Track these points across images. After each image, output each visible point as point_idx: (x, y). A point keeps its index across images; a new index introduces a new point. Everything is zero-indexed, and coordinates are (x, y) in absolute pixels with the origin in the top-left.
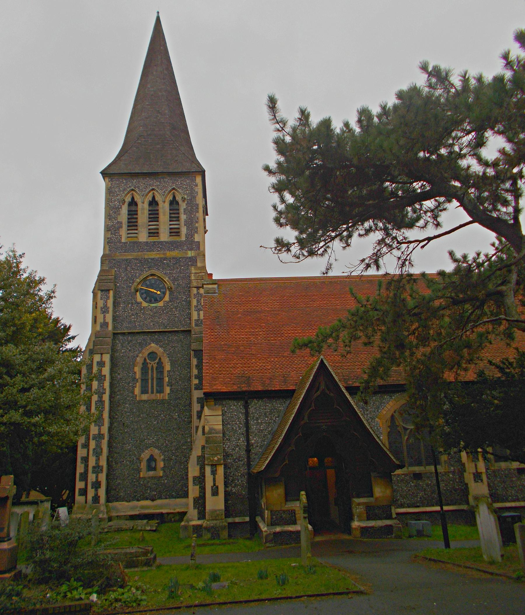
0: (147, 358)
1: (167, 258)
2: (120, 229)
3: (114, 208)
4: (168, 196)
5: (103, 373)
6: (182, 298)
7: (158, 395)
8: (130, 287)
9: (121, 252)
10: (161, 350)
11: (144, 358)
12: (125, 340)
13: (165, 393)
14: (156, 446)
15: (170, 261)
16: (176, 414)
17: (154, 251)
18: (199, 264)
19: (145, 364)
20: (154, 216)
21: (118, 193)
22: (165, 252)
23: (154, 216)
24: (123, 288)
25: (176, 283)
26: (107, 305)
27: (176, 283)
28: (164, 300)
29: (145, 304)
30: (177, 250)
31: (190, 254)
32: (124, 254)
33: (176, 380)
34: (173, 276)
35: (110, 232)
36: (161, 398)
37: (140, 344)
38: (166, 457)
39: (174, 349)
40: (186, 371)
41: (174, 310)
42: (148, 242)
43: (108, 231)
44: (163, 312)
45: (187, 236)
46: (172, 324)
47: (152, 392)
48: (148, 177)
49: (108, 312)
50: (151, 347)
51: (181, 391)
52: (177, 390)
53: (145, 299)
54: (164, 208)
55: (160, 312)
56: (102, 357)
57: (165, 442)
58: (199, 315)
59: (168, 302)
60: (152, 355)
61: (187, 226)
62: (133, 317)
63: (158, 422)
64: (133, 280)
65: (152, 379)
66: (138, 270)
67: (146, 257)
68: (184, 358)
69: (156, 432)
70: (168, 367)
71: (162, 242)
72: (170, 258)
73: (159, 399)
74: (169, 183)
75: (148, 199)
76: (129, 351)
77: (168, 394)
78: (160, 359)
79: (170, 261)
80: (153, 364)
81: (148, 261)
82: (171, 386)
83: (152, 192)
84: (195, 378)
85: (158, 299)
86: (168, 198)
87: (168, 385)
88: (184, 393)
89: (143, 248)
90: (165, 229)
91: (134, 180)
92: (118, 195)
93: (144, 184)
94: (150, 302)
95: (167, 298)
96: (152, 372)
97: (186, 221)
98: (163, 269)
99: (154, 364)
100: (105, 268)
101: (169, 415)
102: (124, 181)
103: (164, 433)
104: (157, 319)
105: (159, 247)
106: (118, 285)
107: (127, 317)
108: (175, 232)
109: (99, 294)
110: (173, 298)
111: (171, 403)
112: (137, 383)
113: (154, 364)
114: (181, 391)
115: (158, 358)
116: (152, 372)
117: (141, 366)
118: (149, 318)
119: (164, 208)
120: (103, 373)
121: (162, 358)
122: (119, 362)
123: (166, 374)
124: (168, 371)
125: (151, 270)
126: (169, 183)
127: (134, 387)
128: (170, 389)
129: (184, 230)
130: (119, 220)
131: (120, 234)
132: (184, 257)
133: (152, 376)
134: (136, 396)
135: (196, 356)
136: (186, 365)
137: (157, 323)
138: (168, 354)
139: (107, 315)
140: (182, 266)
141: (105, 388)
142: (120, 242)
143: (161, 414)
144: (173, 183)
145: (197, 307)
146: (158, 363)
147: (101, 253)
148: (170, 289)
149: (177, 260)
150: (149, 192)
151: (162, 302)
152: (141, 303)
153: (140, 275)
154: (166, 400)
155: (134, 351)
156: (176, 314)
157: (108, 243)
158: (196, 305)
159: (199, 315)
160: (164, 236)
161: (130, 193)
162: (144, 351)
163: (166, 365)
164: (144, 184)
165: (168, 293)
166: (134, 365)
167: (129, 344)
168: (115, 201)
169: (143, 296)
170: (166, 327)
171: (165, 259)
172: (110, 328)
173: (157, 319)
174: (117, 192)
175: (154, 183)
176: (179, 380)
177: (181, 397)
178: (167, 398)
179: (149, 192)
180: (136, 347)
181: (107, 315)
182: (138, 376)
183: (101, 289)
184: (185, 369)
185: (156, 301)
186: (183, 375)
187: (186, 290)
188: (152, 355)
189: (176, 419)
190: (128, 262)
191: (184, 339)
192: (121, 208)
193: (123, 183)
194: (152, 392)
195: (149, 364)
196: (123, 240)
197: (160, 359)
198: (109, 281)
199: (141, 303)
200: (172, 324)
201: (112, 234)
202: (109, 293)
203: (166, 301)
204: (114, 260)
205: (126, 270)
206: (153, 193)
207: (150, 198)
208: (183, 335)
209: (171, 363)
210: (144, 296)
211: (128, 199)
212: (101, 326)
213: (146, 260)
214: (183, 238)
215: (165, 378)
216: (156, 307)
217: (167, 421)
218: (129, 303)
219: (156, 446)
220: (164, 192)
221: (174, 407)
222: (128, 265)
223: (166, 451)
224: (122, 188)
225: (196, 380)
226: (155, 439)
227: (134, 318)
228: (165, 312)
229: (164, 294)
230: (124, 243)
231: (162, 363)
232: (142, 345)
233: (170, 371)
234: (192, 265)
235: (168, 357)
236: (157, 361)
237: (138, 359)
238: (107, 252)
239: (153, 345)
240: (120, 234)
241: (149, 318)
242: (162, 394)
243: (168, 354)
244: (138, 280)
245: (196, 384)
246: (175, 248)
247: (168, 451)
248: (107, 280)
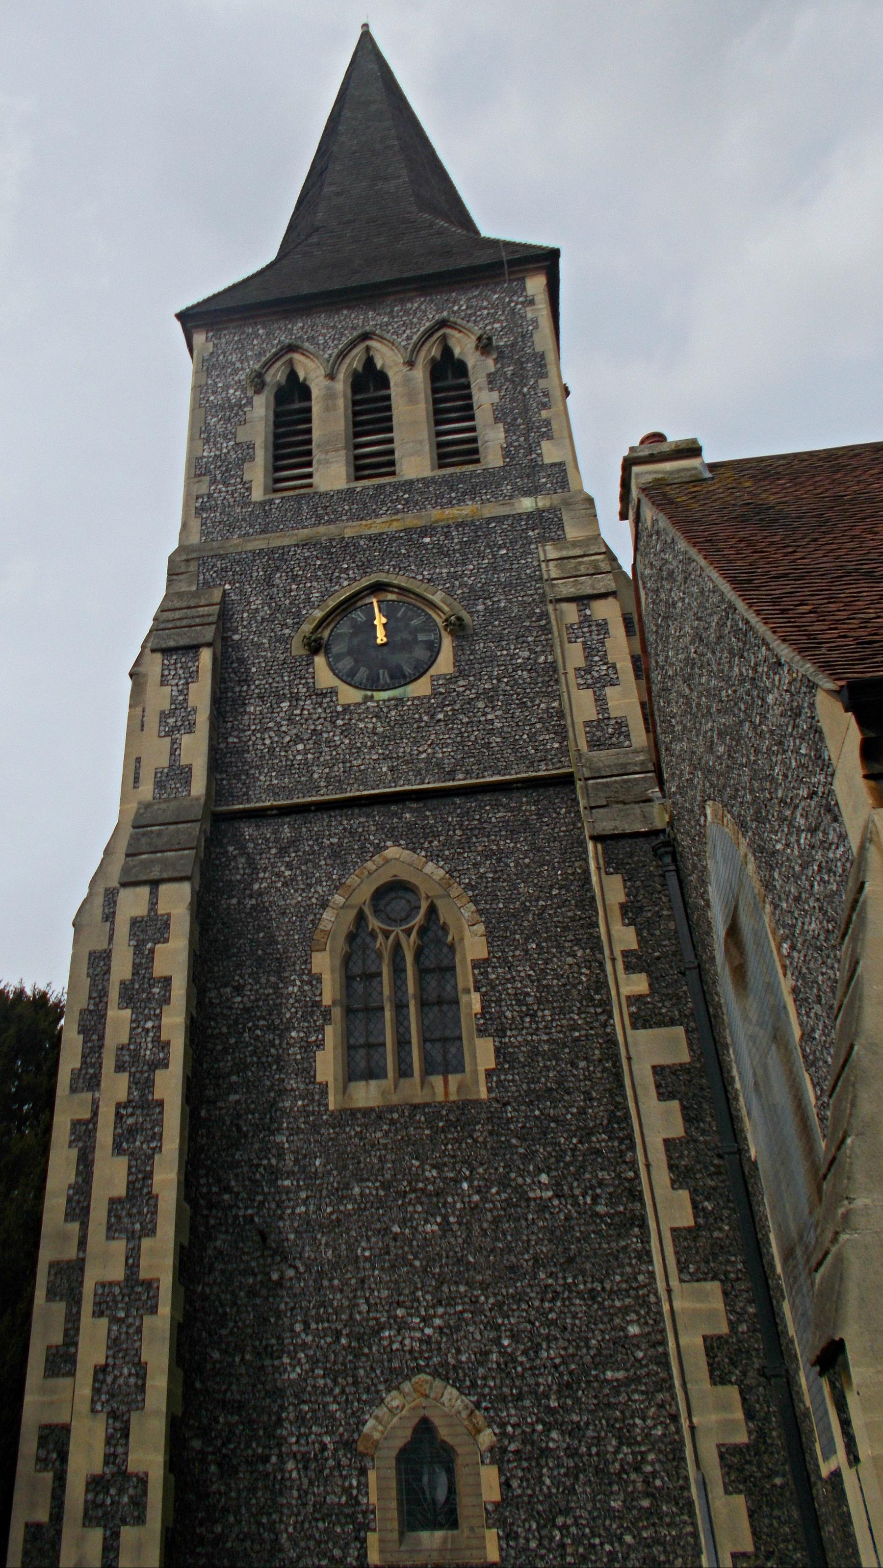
0: (367, 911)
1: (434, 528)
2: (246, 465)
3: (223, 408)
4: (425, 348)
5: (159, 969)
6: (513, 657)
7: (437, 1081)
8: (287, 640)
9: (247, 534)
11: (352, 913)
12: (267, 840)
13: (468, 1068)
14: (444, 1364)
15: (447, 535)
16: (544, 1178)
17: (377, 516)
18: (572, 533)
21: (238, 365)
22: (424, 513)
24: (259, 646)
25: (481, 607)
26: (185, 700)
27: (481, 607)
28: (433, 671)
29: (349, 695)
30: (473, 499)
32: (262, 536)
33: (519, 1003)
34: (463, 585)
35: (207, 478)
36: (453, 1097)
37: (336, 853)
38: (512, 1438)
39: (499, 860)
40: (570, 960)
41: (481, 705)
42: (354, 490)
43: (200, 475)
44: (432, 717)
45: (506, 453)
46: (479, 762)
47: (404, 1072)
48: (348, 308)
49: (191, 728)
50: (387, 861)
51: (556, 1057)
52: (534, 1053)
53: (348, 678)
55: (421, 720)
56: (154, 894)
57: (497, 1341)
59: (451, 680)
61: (505, 423)
62: (300, 747)
63: (445, 1226)
64: (298, 614)
65: (400, 1007)
66: (317, 578)
67: (348, 533)
68: (552, 897)
69: (441, 1281)
71: (411, 482)
72: (448, 526)
73: (440, 1097)
75: (351, 364)
76: (285, 884)
77: (489, 1073)
78: (432, 910)
79: (447, 535)
81: (356, 546)
82: (501, 1032)
83: (362, 346)
84: (629, 968)
85: (408, 670)
86: (423, 353)
87: (482, 1032)
88: (573, 1065)
89: (335, 511)
90: (421, 442)
91: (294, 324)
92: (236, 372)
93: (334, 327)
94: (374, 684)
95: (445, 663)
96: (398, 970)
97: (496, 408)
98: (421, 564)
99: (403, 937)
100: (183, 586)
101: (504, 1184)
102: (261, 331)
103: (484, 1286)
104: (405, 748)
105: (398, 500)
106: (236, 637)
107: (271, 750)
109: (155, 665)
110: (470, 663)
111: (509, 1121)
112: (329, 1030)
113: (403, 937)
114: (556, 1057)
115: (424, 905)
116: (398, 970)
117: (340, 943)
118: (373, 747)
120: (159, 969)
121: (439, 903)
122: (240, 935)
123: (465, 976)
124: (476, 964)
125: (372, 572)
126: (425, 312)
127: (310, 1048)
128: (497, 1051)
130: (238, 441)
131: (246, 478)
132: (506, 517)
134: (324, 1089)
135: (612, 864)
136: (566, 928)
137: (407, 763)
138: (469, 886)
139: (186, 740)
140: (500, 548)
141: (163, 1038)
142: (245, 502)
143: (457, 1181)
144: (439, 310)
145: (588, 671)
146: (423, 931)
147: (173, 545)
148: (457, 628)
150: (353, 344)
151: (425, 680)
152: (333, 692)
153: (326, 595)
154: (477, 1102)
155: (310, 886)
156: (491, 722)
157: (199, 510)
158: (581, 662)
161: (284, 359)
162: (352, 880)
163: (467, 934)
164: (334, 327)
165: (447, 643)
166: (310, 944)
167: (283, 851)
168: (226, 388)
169: (340, 665)
170: (452, 775)
171: (425, 531)
172: (199, 786)
173: (405, 748)
174: (234, 364)
176: (539, 1001)
177: (559, 1083)
178: (483, 1094)
179: (353, 344)
180: (317, 866)
181: (186, 740)
182: (329, 993)
183: (164, 646)
184: (559, 946)
185: (400, 678)
186: (558, 977)
187: (527, 628)
189: (543, 1207)
191: (540, 816)
192: (250, 402)
193: (257, 336)
194: (404, 1072)
195: (380, 938)
196: (258, 494)
198: (198, 620)
199: (333, 692)
200: (479, 762)
201: (214, 481)
202: (196, 658)
203: (439, 677)
204: (222, 557)
205: (269, 582)
206: (368, 349)
207: (355, 359)
208: (536, 803)
209: (487, 923)
210: (347, 664)
211: (275, 375)
212: (160, 785)
213: (348, 546)
215: (464, 999)
216: (400, 701)
217: (496, 1221)
218: (280, 698)
219: (444, 1364)
220: (409, 338)
221: (522, 1139)
222: (278, 569)
223: (503, 1399)
224: (252, 350)
225: (634, 977)
226: (438, 1322)
227: (306, 752)
228: (440, 716)
229: (434, 650)
230: (263, 504)
231: (444, 928)
233: (486, 960)
234: (543, 539)
235: (474, 900)
236: (418, 919)
237: (328, 915)
238: (195, 539)
239: (392, 852)
240: (246, 478)
241: (373, 747)
242: (454, 1080)
243: (469, 886)
244: (319, 614)
245: (635, 1000)
246: (464, 494)
247: (520, 1397)
248: (193, 617)
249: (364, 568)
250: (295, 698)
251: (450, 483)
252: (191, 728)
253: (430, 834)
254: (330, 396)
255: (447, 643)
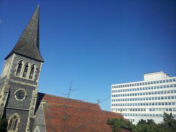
10: (18, 115)
19: (12, 120)
20: (26, 70)
23: (26, 70)
29: (17, 99)
31: (34, 86)
49: (5, 100)
53: (17, 97)
54: (29, 68)
58: (33, 107)
59: (24, 100)
60: (15, 117)
67: (21, 83)
70: (19, 121)
74: (33, 62)
78: (17, 118)
80: (15, 120)
95: (24, 99)
108: (30, 77)
119: (29, 68)
123: (18, 124)
129: (34, 78)
133: (13, 124)
139: (4, 101)
149: (30, 87)
159: (33, 107)
160: (27, 78)
171: (27, 86)
172: (4, 106)
175: (30, 60)
181: (4, 101)
185: (21, 99)
188: (15, 117)
190: (15, 84)
197: (17, 118)
214: (33, 80)
229: (24, 97)
232: (13, 113)
249: (22, 87)
250: (13, 98)
251: (30, 81)
252: (5, 100)
253: (19, 112)
254: (23, 67)
255: (25, 97)
